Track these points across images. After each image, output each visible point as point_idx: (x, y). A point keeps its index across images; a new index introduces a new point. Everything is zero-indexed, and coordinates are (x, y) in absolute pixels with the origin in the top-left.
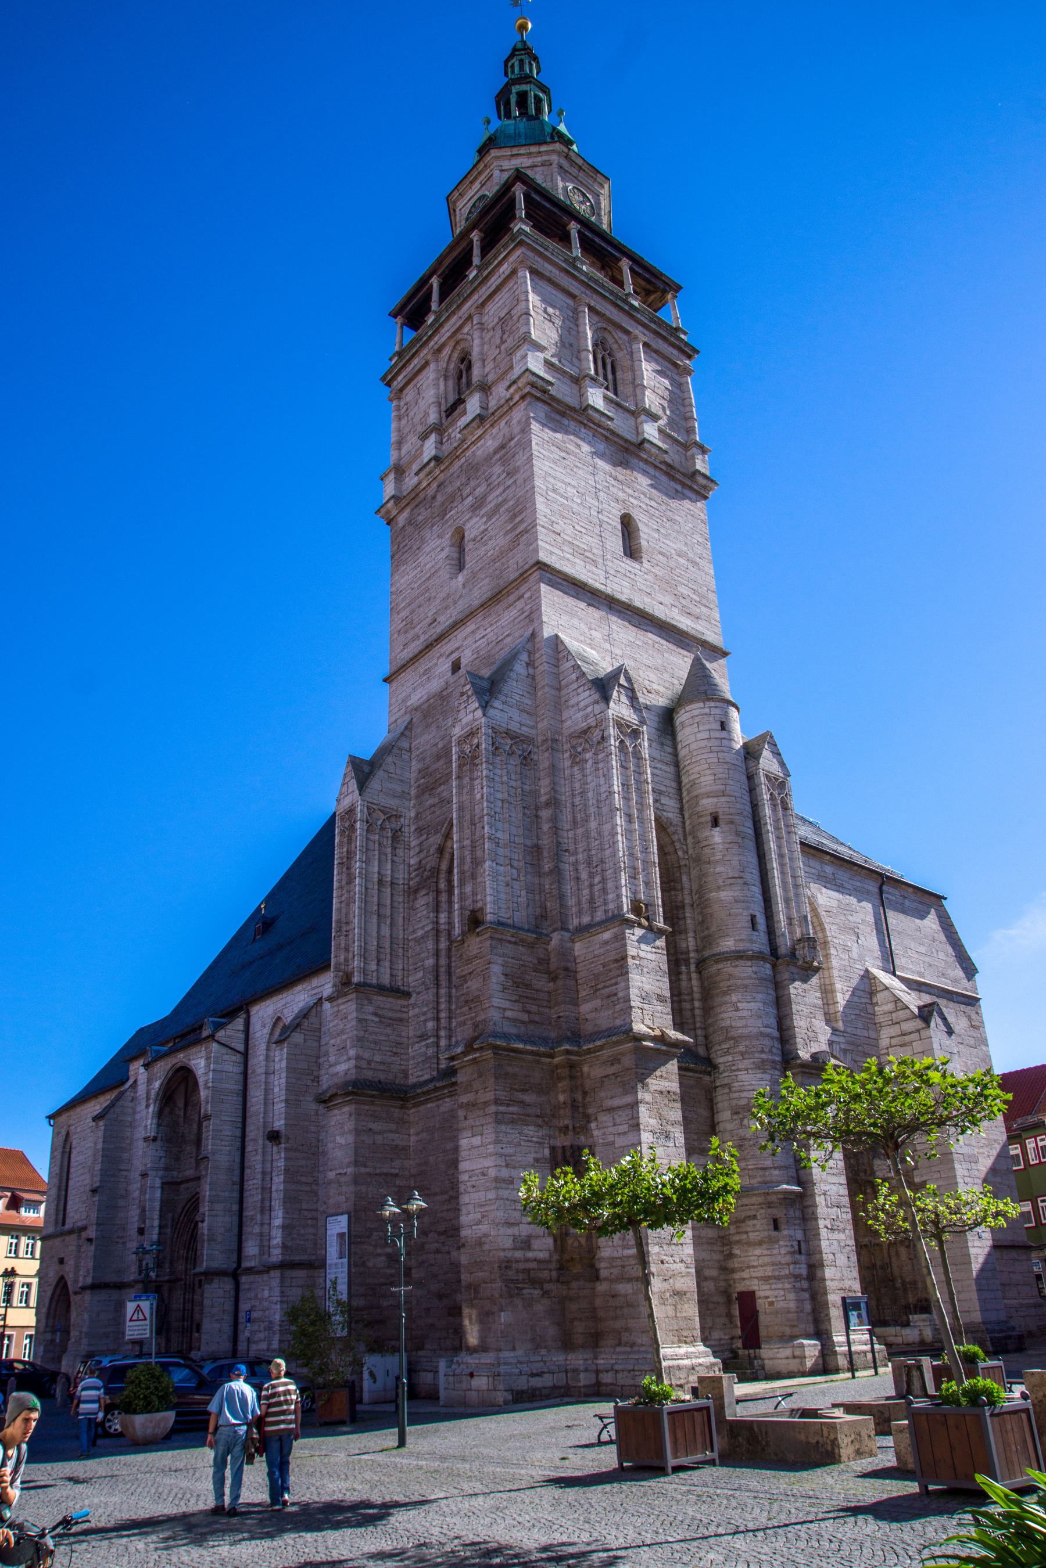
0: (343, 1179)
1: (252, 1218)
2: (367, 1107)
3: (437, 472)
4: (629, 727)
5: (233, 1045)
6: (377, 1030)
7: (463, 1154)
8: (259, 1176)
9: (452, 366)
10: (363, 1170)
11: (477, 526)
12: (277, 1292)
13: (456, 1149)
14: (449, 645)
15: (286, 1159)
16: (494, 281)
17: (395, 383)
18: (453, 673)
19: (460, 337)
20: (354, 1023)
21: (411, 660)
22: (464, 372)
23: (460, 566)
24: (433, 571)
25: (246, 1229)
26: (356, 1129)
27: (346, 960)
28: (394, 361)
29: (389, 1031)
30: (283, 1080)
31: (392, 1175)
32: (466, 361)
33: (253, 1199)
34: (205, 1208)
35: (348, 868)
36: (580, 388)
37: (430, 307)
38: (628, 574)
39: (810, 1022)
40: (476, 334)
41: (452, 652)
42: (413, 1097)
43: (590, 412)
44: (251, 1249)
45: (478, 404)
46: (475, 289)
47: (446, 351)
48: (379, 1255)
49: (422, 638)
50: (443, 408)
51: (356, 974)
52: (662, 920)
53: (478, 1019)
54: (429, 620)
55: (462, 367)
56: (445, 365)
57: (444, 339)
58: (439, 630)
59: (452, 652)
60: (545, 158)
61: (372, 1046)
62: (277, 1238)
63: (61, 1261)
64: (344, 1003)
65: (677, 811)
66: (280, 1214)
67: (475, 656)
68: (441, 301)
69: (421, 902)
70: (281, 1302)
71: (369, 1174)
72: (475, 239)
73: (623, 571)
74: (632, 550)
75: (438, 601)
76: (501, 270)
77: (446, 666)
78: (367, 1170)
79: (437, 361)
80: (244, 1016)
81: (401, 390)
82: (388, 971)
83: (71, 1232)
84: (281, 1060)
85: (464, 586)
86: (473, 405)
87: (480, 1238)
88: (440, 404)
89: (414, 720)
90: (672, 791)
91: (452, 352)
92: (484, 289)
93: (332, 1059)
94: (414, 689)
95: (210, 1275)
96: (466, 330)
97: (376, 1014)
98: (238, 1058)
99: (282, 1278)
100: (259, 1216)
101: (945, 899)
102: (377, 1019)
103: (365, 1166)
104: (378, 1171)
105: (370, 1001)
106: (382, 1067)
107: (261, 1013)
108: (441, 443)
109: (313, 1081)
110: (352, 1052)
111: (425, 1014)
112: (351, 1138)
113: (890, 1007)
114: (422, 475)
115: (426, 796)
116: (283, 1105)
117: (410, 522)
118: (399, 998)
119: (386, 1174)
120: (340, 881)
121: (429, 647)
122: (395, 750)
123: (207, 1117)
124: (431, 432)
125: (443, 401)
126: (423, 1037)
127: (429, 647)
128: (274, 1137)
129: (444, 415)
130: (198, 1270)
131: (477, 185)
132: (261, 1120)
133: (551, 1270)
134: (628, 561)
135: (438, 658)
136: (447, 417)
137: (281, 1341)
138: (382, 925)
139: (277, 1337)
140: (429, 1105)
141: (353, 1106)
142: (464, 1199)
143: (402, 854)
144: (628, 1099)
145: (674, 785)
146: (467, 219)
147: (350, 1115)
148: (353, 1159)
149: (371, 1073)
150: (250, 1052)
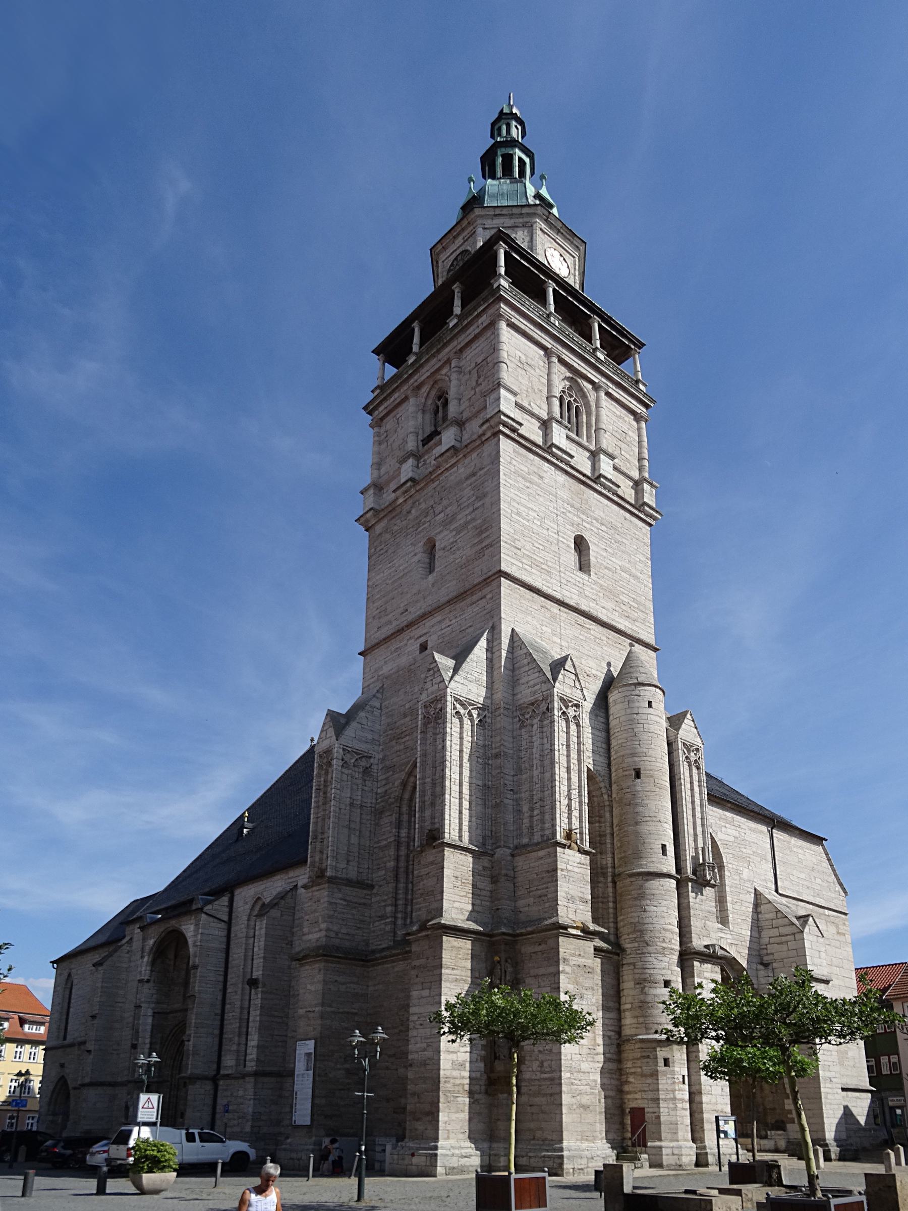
0: (311, 1015)
1: (231, 1040)
2: (334, 965)
3: (413, 491)
4: (570, 702)
5: (219, 916)
6: (345, 911)
7: (414, 1001)
8: (238, 1010)
9: (429, 402)
10: (329, 1009)
11: (447, 538)
12: (251, 1091)
13: (408, 997)
14: (418, 630)
15: (262, 998)
16: (473, 331)
17: (376, 413)
18: (421, 652)
19: (439, 377)
20: (326, 905)
21: (384, 639)
22: (440, 408)
23: (431, 569)
24: (406, 571)
25: (224, 1047)
26: (324, 981)
27: (321, 859)
28: (376, 394)
29: (354, 911)
30: (262, 943)
31: (352, 1013)
32: (443, 398)
33: (232, 1025)
34: (190, 1031)
35: (325, 793)
36: (546, 429)
37: (411, 348)
38: (577, 584)
39: (705, 923)
40: (454, 376)
41: (421, 637)
42: (373, 960)
43: (554, 450)
44: (229, 1061)
45: (453, 436)
46: (455, 336)
47: (425, 389)
48: (340, 1069)
49: (395, 623)
50: (421, 438)
51: (328, 870)
52: (588, 844)
53: (431, 907)
54: (401, 610)
55: (439, 403)
56: (423, 401)
57: (423, 378)
58: (410, 618)
59: (421, 637)
60: (526, 220)
61: (341, 922)
62: (252, 1054)
63: (62, 1066)
64: (317, 890)
65: (605, 765)
66: (256, 1037)
67: (441, 641)
68: (421, 345)
69: (385, 820)
70: (254, 1099)
71: (333, 1012)
72: (456, 291)
73: (574, 582)
74: (584, 566)
75: (409, 595)
76: (480, 321)
77: (417, 646)
78: (333, 1009)
79: (416, 396)
80: (229, 895)
81: (382, 419)
82: (356, 869)
83: (71, 1045)
84: (261, 929)
85: (433, 585)
86: (448, 437)
87: (425, 1060)
88: (417, 434)
89: (385, 686)
90: (602, 750)
91: (431, 389)
92: (463, 336)
93: (305, 930)
94: (386, 662)
95: (194, 1079)
96: (444, 372)
97: (345, 900)
98: (223, 926)
99: (256, 1083)
100: (236, 1038)
101: (826, 840)
102: (345, 903)
103: (330, 1006)
104: (341, 1010)
105: (340, 890)
106: (347, 937)
107: (243, 894)
108: (418, 467)
109: (287, 944)
110: (323, 926)
111: (385, 901)
112: (320, 987)
113: (773, 915)
114: (399, 492)
115: (394, 743)
116: (262, 960)
117: (386, 530)
118: (364, 889)
119: (348, 1013)
120: (317, 802)
121: (400, 631)
122: (368, 708)
123: (195, 967)
124: (408, 457)
125: (421, 431)
126: (383, 917)
127: (400, 631)
128: (253, 983)
129: (420, 444)
130: (183, 1075)
131: (460, 240)
132: (241, 970)
133: (481, 1086)
134: (579, 574)
135: (408, 640)
136: (424, 445)
137: (252, 1127)
138: (352, 836)
139: (249, 1123)
140: (386, 966)
141: (323, 964)
142: (412, 1033)
143: (370, 785)
144: (552, 969)
145: (604, 746)
146: (449, 270)
147: (320, 970)
148: (320, 1001)
149: (338, 941)
150: (233, 921)
